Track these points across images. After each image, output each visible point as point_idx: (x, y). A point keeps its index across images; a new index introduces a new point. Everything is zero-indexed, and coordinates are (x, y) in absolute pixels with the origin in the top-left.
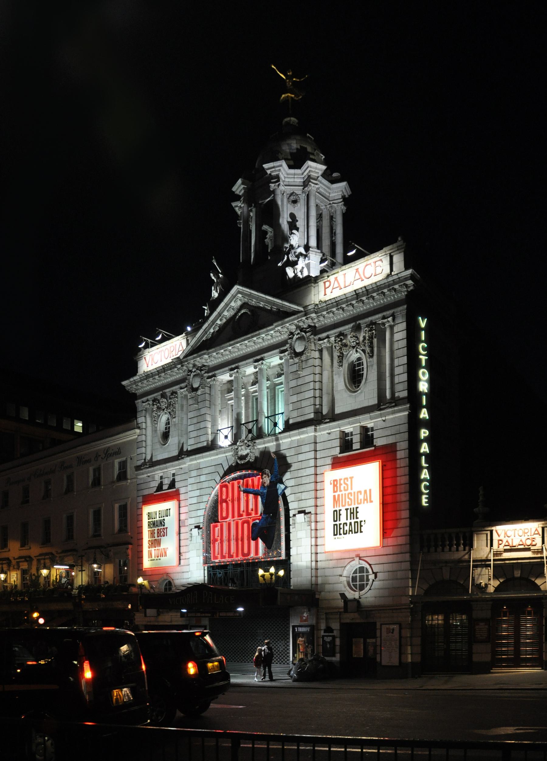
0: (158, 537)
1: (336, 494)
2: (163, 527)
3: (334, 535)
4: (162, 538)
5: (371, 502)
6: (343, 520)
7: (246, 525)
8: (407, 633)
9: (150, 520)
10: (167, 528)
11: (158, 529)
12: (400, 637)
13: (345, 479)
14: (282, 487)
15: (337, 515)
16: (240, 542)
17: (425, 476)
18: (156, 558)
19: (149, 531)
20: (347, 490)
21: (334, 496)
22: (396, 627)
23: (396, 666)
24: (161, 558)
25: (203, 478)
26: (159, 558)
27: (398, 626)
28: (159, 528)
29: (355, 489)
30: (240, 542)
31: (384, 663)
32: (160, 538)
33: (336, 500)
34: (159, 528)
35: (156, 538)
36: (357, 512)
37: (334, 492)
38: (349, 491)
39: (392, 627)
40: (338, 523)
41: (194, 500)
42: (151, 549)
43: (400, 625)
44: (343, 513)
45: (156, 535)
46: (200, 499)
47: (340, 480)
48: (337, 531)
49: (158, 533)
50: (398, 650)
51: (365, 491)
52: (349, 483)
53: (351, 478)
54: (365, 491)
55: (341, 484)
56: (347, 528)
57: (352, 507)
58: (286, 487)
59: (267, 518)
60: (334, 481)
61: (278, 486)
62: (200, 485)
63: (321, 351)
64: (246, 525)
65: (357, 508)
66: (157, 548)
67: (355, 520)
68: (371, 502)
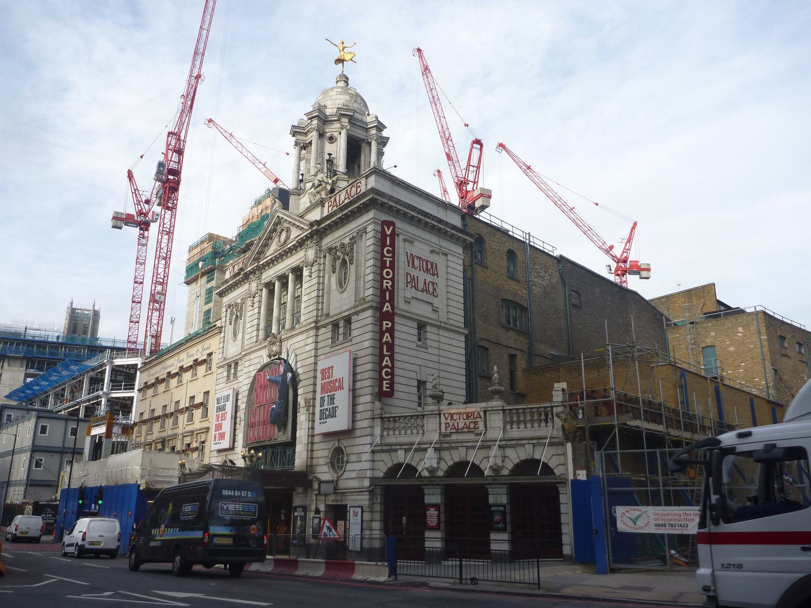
5: (343, 389)
8: (367, 516)
12: (362, 521)
17: (387, 364)
22: (359, 510)
27: (360, 509)
29: (334, 378)
36: (334, 398)
37: (322, 380)
38: (331, 379)
40: (322, 408)
43: (362, 508)
44: (326, 399)
47: (326, 369)
52: (331, 371)
53: (332, 367)
55: (326, 373)
56: (327, 413)
59: (280, 403)
60: (323, 369)
63: (325, 257)
65: (334, 394)
67: (334, 406)
68: (343, 389)
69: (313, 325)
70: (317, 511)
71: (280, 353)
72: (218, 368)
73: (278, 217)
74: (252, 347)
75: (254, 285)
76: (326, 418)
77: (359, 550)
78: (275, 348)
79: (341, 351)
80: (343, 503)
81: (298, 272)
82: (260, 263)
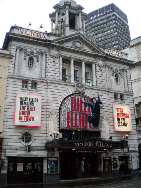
0: (28, 110)
1: (118, 113)
2: (32, 106)
3: (118, 126)
4: (31, 112)
5: (129, 118)
6: (121, 121)
7: (85, 115)
9: (22, 101)
10: (35, 107)
11: (28, 107)
13: (120, 109)
14: (102, 105)
15: (118, 120)
16: (82, 122)
18: (26, 121)
19: (21, 106)
20: (121, 112)
21: (117, 113)
22: (136, 157)
23: (136, 170)
24: (30, 121)
25: (57, 91)
26: (28, 121)
28: (29, 106)
29: (124, 113)
30: (82, 122)
31: (133, 169)
32: (29, 111)
33: (118, 115)
34: (29, 106)
35: (26, 110)
36: (125, 120)
38: (122, 113)
39: (134, 157)
41: (52, 99)
42: (21, 115)
44: (121, 119)
45: (26, 109)
46: (55, 99)
47: (119, 108)
48: (119, 124)
49: (28, 108)
50: (137, 164)
51: (127, 114)
52: (122, 110)
53: (122, 109)
54: (127, 114)
55: (119, 110)
56: (122, 124)
57: (123, 118)
58: (103, 106)
60: (117, 108)
61: (100, 104)
62: (54, 93)
64: (85, 115)
66: (27, 116)
68: (129, 118)
69: (108, 90)
70: (115, 158)
71: (84, 92)
72: (9, 77)
73: (79, 36)
74: (58, 82)
75: (54, 52)
76: (122, 126)
77: (137, 169)
78: (80, 90)
79: (120, 104)
80: (127, 155)
81: (89, 65)
82: (65, 47)
